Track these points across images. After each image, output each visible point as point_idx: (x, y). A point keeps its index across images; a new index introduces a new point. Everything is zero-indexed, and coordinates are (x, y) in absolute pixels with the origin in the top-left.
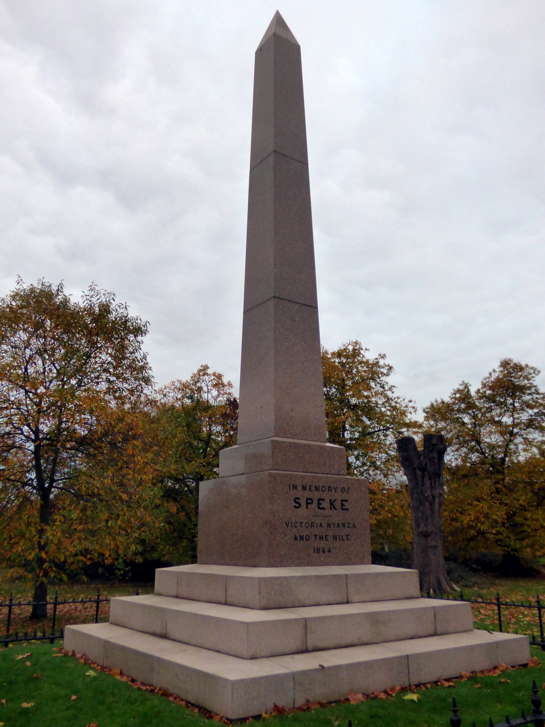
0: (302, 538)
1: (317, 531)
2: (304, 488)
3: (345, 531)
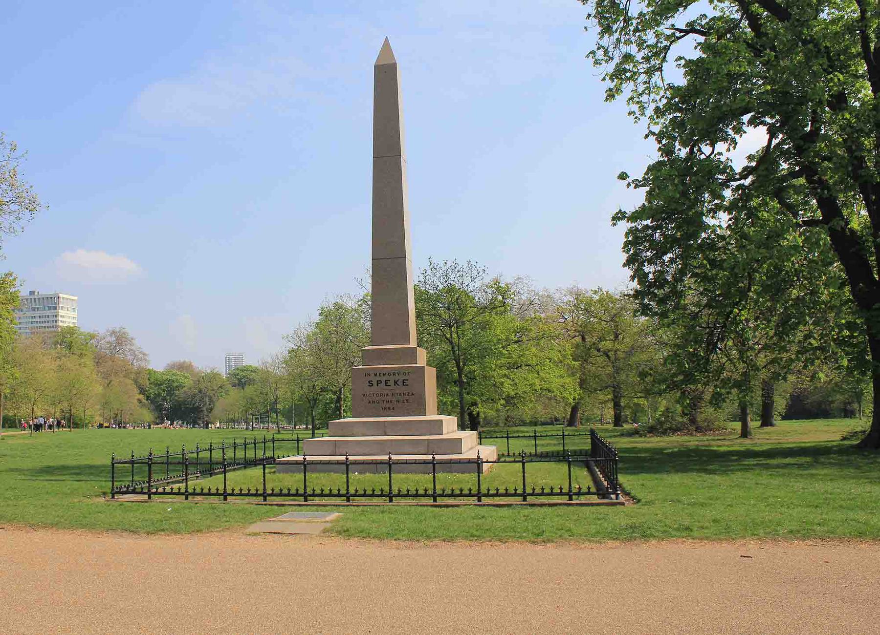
0: (374, 402)
2: (376, 375)
3: (407, 397)
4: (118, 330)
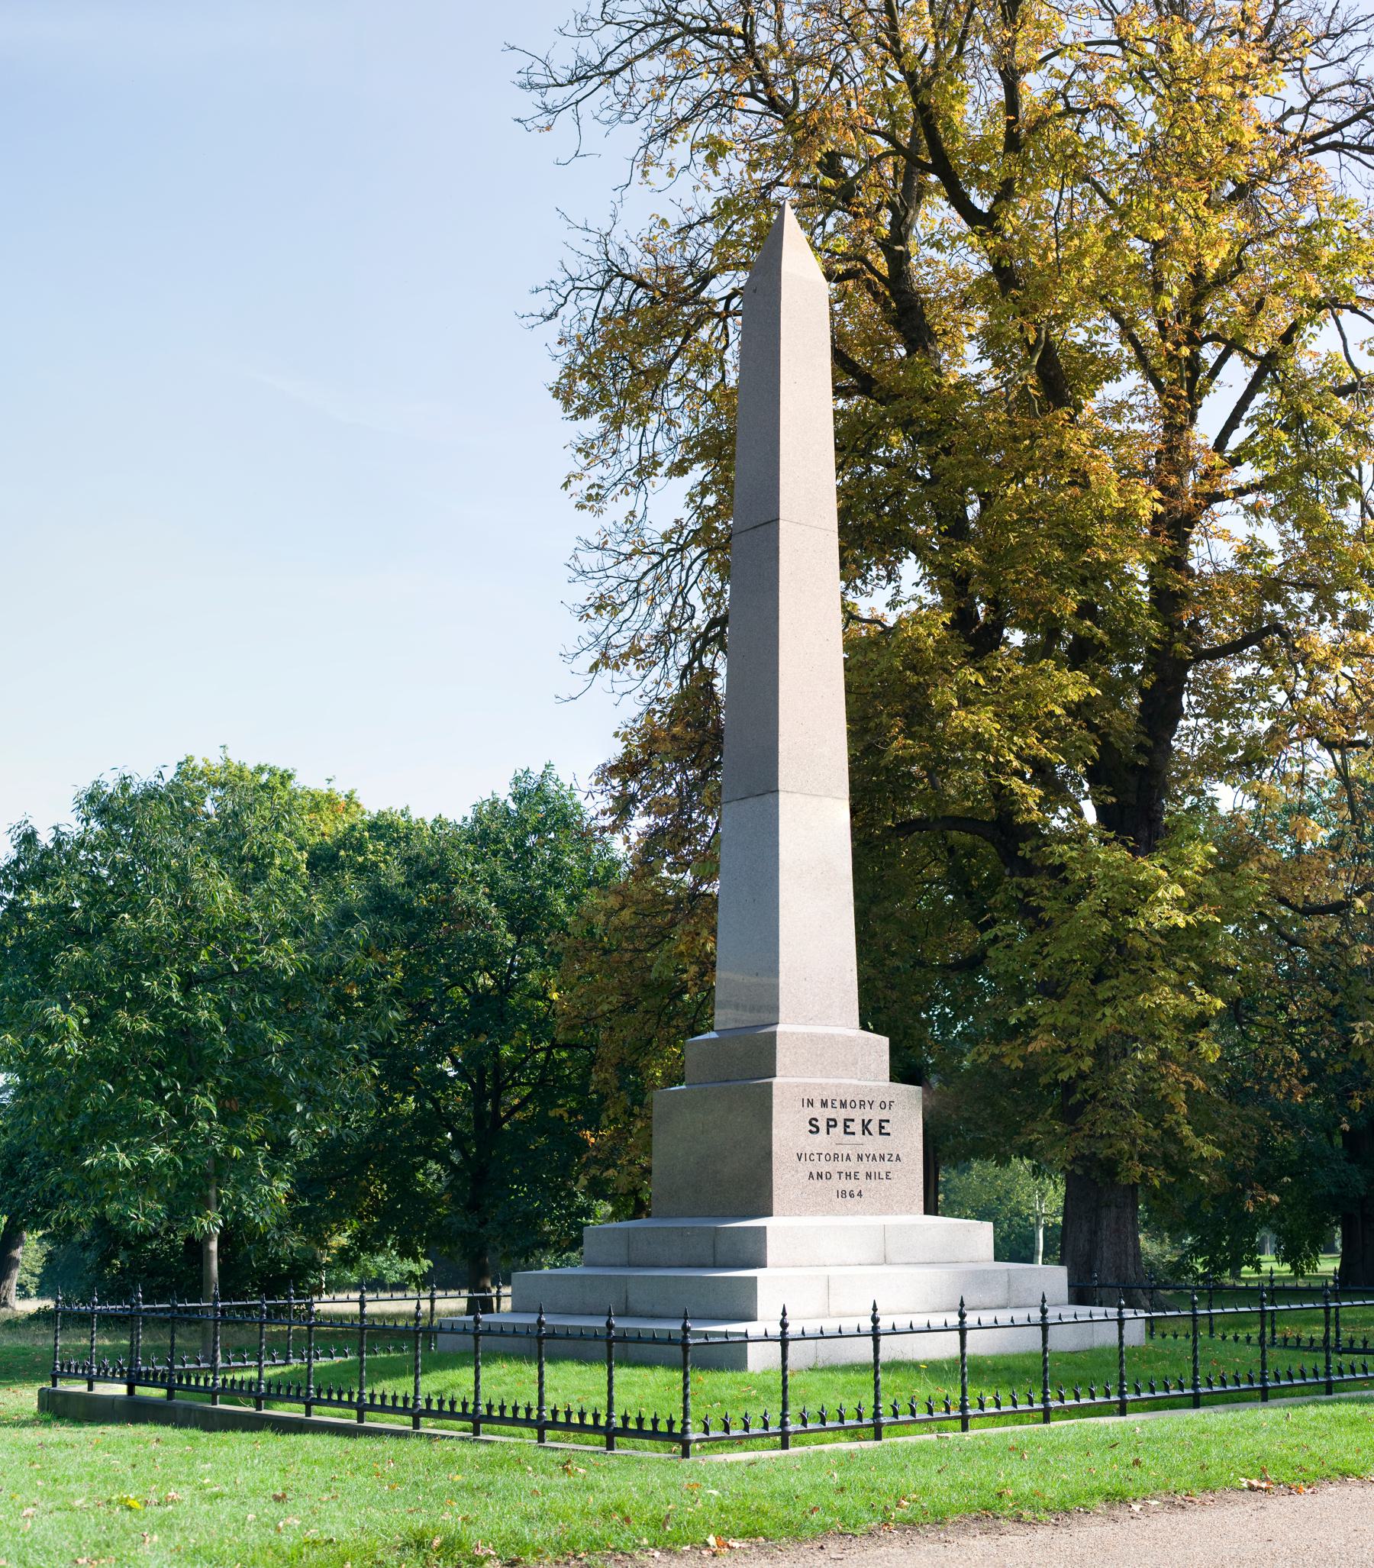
0: (820, 1176)
1: (842, 1166)
2: (824, 1104)
3: (886, 1166)
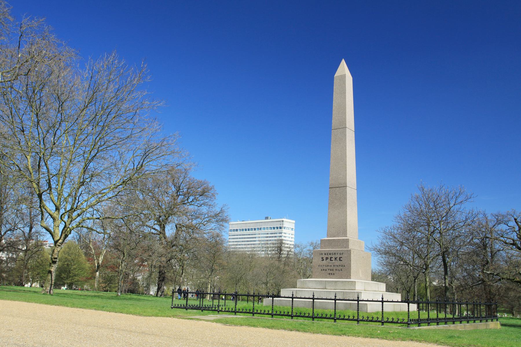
1: (329, 268)
2: (325, 254)
4: (315, 242)
